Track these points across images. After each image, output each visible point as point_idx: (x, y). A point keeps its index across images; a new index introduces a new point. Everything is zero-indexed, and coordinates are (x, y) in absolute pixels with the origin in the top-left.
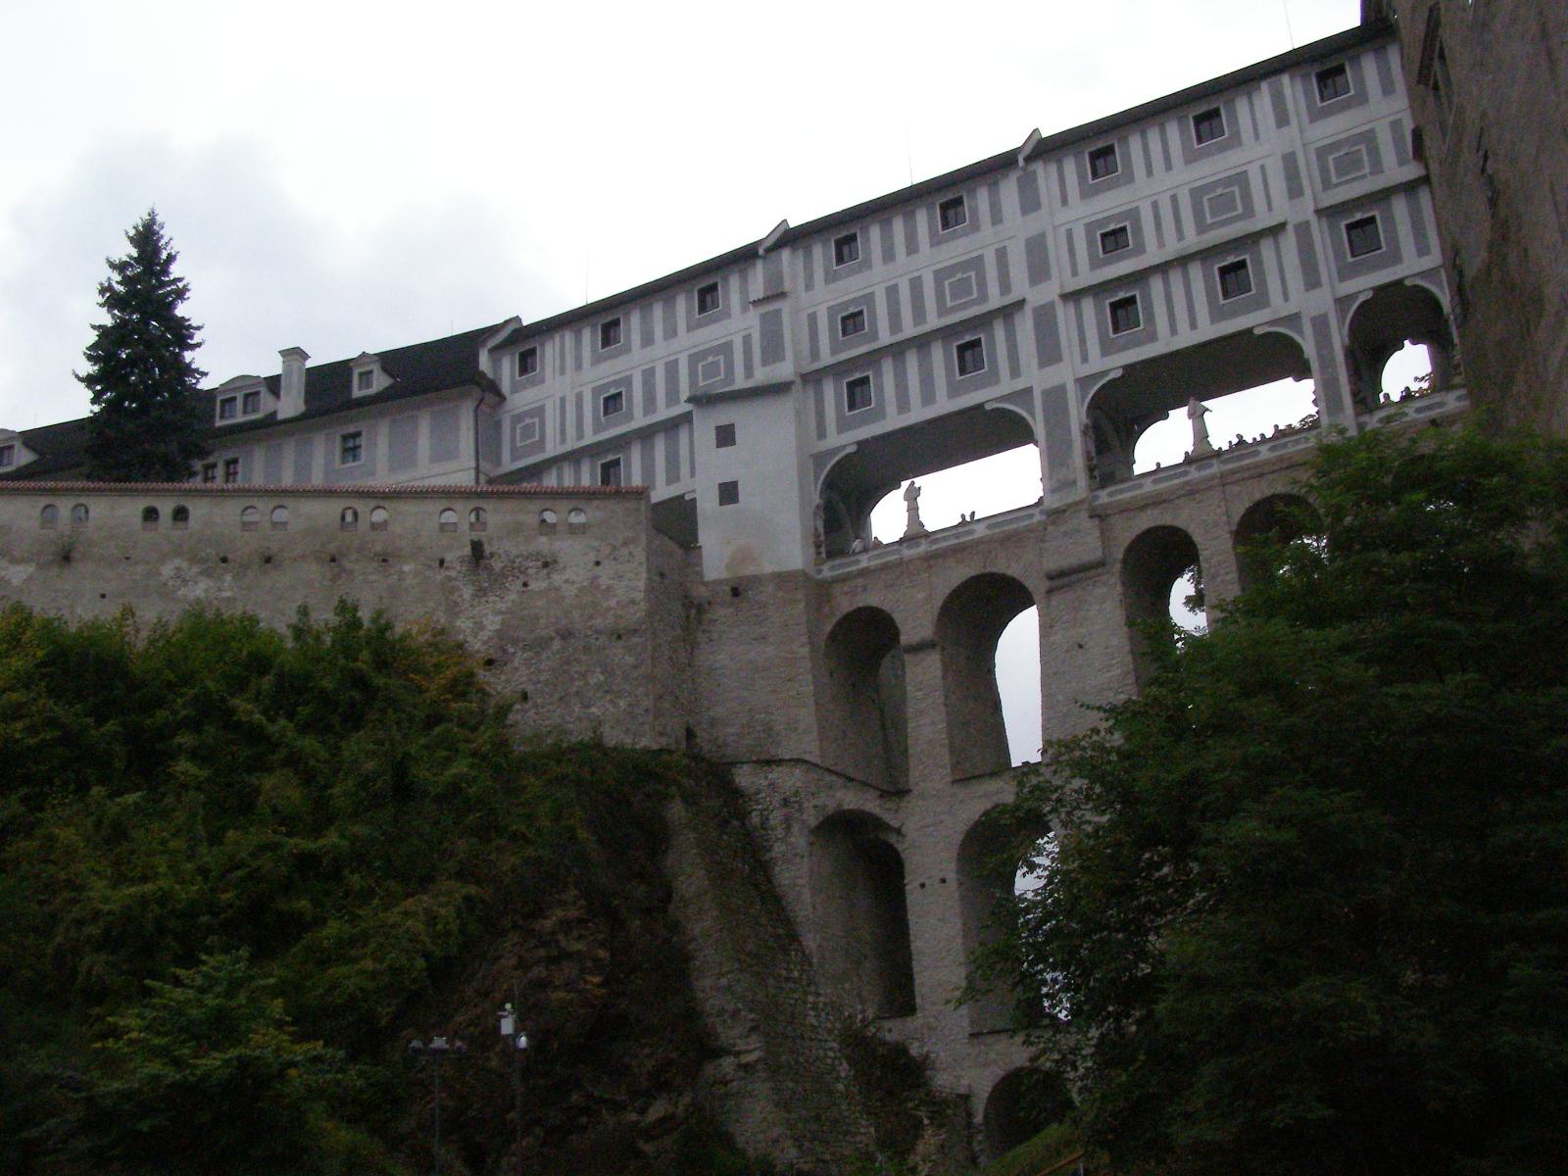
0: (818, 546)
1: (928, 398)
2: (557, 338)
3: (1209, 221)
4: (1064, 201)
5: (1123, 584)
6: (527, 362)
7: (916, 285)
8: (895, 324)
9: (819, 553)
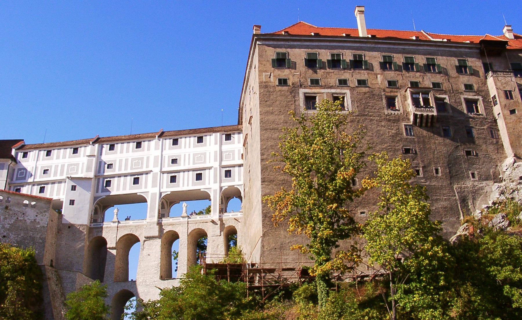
0: (91, 219)
1: (124, 189)
2: (34, 151)
3: (196, 162)
4: (165, 150)
5: (161, 242)
6: (25, 155)
7: (127, 160)
8: (120, 169)
9: (91, 220)
